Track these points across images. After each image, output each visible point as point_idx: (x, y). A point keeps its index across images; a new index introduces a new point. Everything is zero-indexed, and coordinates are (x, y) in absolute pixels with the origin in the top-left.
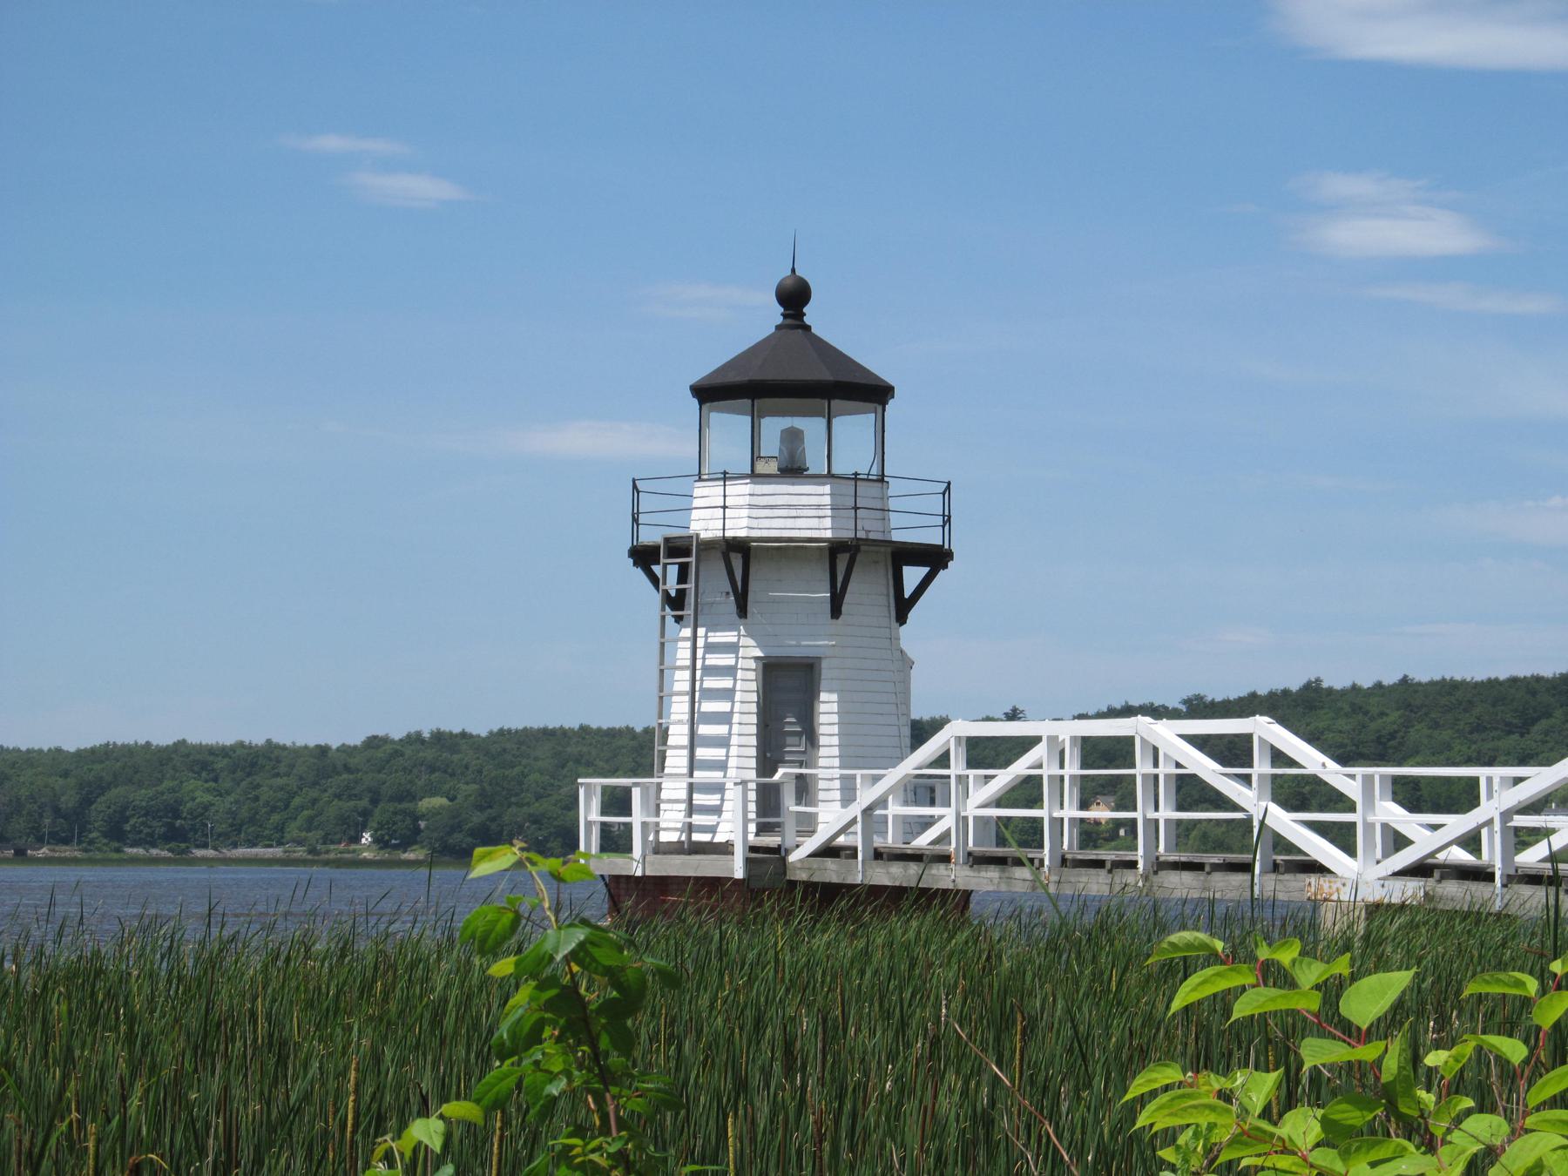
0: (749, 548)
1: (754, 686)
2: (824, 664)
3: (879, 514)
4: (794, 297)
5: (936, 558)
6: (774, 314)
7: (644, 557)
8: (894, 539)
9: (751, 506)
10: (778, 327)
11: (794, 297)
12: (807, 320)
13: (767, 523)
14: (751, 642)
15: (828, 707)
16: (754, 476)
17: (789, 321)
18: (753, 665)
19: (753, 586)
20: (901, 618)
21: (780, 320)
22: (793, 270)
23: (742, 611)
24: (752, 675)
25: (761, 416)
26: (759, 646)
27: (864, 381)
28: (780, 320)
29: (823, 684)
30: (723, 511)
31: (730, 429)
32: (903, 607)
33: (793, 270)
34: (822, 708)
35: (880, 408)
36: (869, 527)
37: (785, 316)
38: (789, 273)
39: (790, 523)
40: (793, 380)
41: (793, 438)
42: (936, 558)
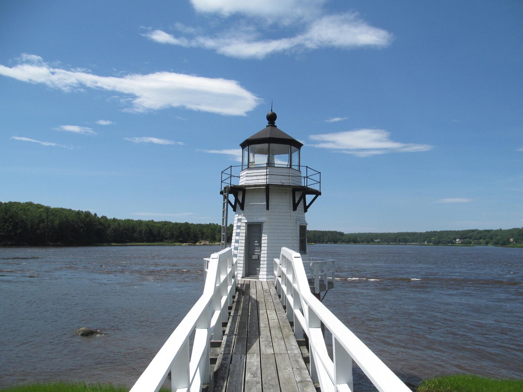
0: (245, 190)
1: (244, 231)
2: (264, 224)
4: (272, 118)
5: (317, 193)
6: (266, 123)
7: (222, 193)
9: (247, 176)
10: (267, 126)
11: (272, 118)
13: (250, 182)
14: (244, 218)
15: (265, 238)
16: (249, 168)
18: (244, 225)
19: (246, 201)
20: (306, 211)
21: (268, 124)
23: (242, 208)
24: (244, 228)
25: (273, 155)
26: (246, 219)
27: (285, 138)
28: (268, 124)
29: (264, 231)
30: (244, 179)
32: (306, 208)
34: (263, 238)
39: (257, 181)
40: (272, 140)
42: (317, 193)
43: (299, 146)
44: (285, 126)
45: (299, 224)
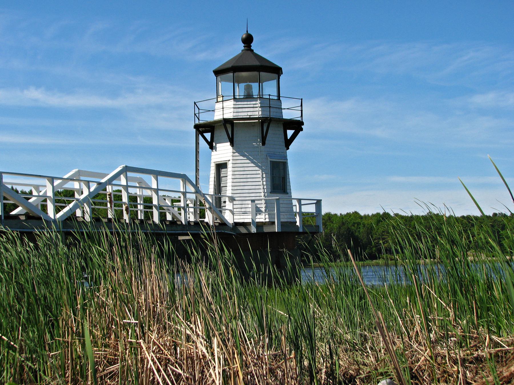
3: (278, 110)
4: (248, 40)
8: (285, 117)
11: (248, 40)
12: (252, 48)
17: (246, 48)
21: (243, 48)
22: (247, 31)
28: (243, 48)
31: (225, 86)
32: (288, 143)
33: (247, 31)
35: (276, 76)
36: (274, 114)
37: (244, 47)
38: (246, 32)
41: (248, 89)
43: (277, 71)
44: (261, 49)
45: (269, 160)
